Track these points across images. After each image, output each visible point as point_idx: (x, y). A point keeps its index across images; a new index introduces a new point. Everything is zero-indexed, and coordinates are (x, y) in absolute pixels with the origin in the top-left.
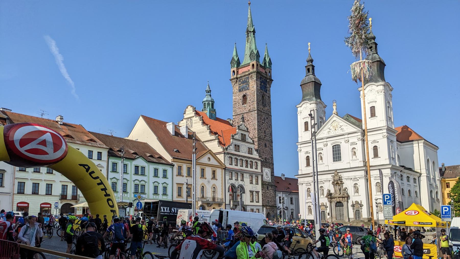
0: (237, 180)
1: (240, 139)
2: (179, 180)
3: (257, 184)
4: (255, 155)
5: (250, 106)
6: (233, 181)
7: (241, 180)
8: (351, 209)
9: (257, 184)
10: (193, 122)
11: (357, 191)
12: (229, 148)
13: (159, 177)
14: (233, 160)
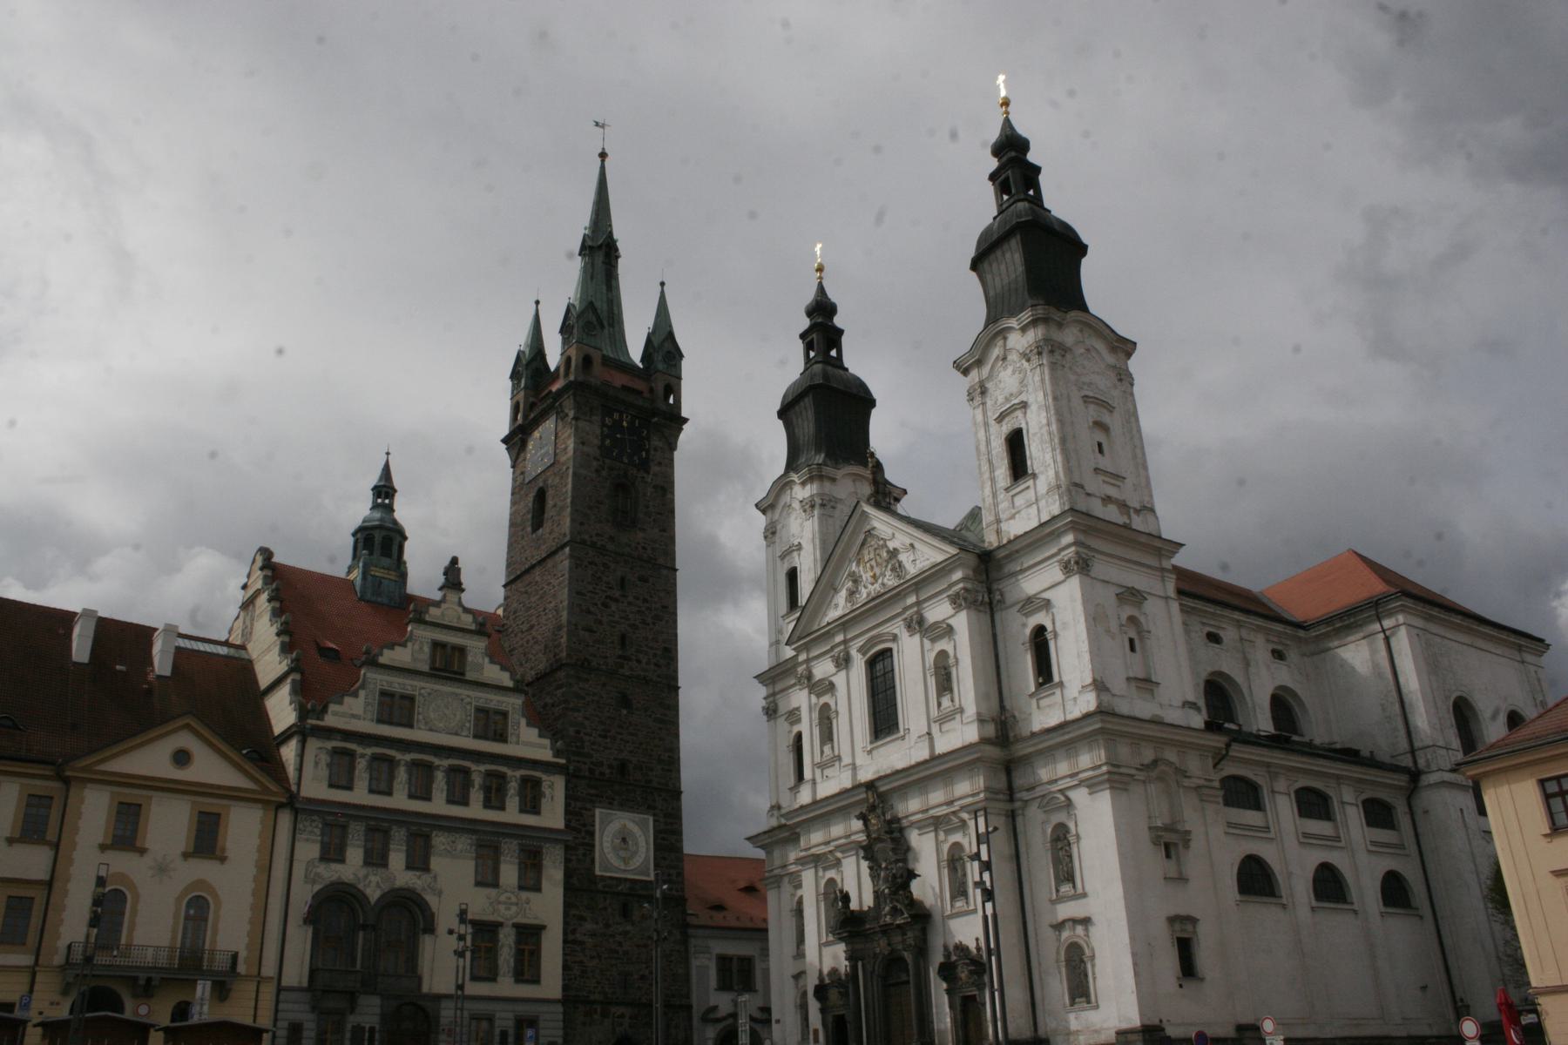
0: (376, 859)
1: (426, 668)
4: (530, 743)
6: (352, 867)
7: (410, 867)
8: (939, 992)
9: (531, 881)
12: (333, 707)
14: (361, 764)
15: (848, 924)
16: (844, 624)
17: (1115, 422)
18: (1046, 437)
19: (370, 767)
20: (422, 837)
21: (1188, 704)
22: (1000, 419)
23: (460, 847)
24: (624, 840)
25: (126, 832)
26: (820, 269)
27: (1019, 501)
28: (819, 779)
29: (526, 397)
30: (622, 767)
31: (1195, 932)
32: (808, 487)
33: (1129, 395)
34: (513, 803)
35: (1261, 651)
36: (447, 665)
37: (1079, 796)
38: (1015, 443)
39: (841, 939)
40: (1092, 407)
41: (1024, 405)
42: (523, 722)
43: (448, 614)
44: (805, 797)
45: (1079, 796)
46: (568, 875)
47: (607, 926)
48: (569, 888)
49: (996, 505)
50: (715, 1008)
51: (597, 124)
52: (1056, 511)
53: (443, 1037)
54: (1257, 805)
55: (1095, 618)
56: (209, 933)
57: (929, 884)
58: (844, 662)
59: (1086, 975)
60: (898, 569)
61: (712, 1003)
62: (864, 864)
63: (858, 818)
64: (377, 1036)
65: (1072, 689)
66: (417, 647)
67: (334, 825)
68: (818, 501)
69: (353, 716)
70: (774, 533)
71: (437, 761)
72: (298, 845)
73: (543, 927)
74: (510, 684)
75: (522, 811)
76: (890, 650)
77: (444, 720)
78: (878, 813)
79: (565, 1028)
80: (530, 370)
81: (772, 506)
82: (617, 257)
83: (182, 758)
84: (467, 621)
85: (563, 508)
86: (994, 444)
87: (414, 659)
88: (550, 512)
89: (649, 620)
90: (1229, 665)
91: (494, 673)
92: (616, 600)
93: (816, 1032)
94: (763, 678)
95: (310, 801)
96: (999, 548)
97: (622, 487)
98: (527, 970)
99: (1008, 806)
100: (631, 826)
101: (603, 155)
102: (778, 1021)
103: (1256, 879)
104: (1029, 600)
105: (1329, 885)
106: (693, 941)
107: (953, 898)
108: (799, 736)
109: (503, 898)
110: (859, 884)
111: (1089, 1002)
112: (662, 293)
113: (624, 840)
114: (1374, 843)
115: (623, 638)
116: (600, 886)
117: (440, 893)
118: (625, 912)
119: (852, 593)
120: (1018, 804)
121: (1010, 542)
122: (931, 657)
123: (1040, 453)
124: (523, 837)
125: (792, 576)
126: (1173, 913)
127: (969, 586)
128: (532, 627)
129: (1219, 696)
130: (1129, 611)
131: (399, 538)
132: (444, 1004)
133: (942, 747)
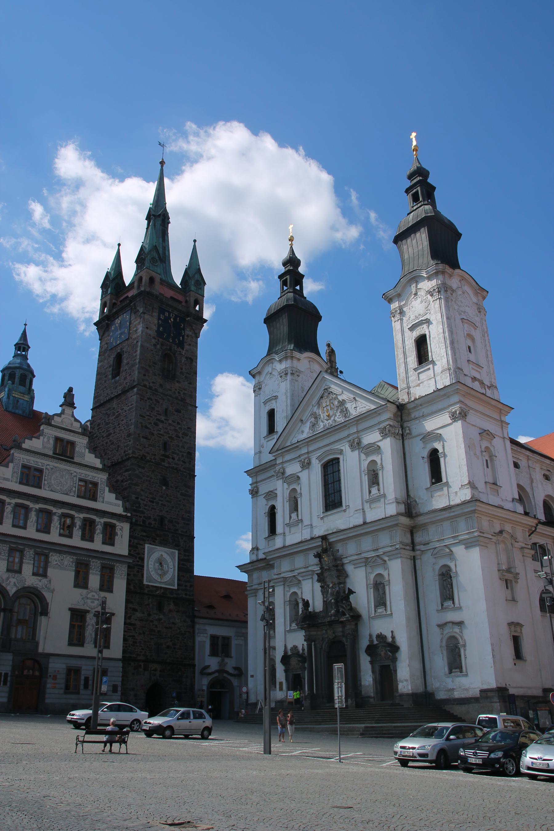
1: (51, 453)
4: (109, 502)
5: (125, 378)
8: (365, 662)
9: (107, 585)
11: (381, 601)
15: (307, 620)
17: (477, 334)
18: (442, 340)
19: (14, 511)
20: (44, 552)
21: (513, 500)
22: (412, 329)
23: (66, 563)
24: (161, 564)
26: (291, 239)
27: (423, 376)
28: (287, 534)
29: (111, 300)
30: (162, 520)
31: (521, 633)
34: (98, 537)
35: (538, 476)
36: (64, 451)
37: (459, 551)
39: (302, 629)
40: (466, 325)
42: (107, 489)
43: (66, 421)
44: (278, 542)
46: (128, 584)
47: (149, 615)
48: (128, 591)
49: (407, 378)
50: (208, 667)
52: (448, 383)
53: (50, 680)
55: (469, 447)
58: (306, 465)
59: (460, 656)
60: (345, 412)
61: (207, 664)
62: (318, 586)
63: (315, 556)
64: (9, 679)
66: (46, 440)
68: (289, 371)
70: (260, 389)
71: (54, 510)
74: (100, 466)
75: (104, 543)
76: (338, 459)
77: (60, 485)
78: (328, 556)
79: (122, 677)
81: (259, 373)
82: (169, 223)
84: (76, 427)
85: (133, 365)
87: (44, 447)
88: (124, 367)
89: (180, 435)
92: (162, 422)
93: (281, 684)
94: (249, 473)
96: (409, 403)
97: (168, 357)
99: (412, 554)
100: (165, 556)
101: (162, 163)
102: (252, 676)
104: (429, 434)
106: (197, 626)
107: (376, 607)
108: (273, 508)
109: (90, 596)
110: (313, 594)
111: (461, 672)
112: (195, 246)
113: (161, 564)
116: (146, 591)
117: (53, 591)
118: (160, 608)
119: (313, 425)
121: (416, 399)
122: (365, 464)
123: (438, 349)
124: (104, 559)
125: (271, 414)
126: (510, 621)
127: (392, 424)
128: (110, 434)
129: (522, 497)
130: (485, 444)
131: (30, 376)
132: (51, 660)
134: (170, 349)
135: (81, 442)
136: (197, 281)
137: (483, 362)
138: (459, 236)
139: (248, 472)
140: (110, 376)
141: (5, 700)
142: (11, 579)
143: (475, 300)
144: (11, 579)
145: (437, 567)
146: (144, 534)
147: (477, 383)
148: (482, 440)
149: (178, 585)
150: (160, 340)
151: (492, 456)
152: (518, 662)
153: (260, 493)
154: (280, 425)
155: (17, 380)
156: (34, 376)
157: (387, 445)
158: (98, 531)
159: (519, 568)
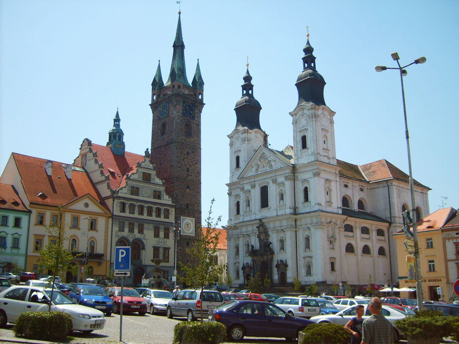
0: (131, 230)
1: (141, 180)
2: (40, 230)
3: (167, 236)
4: (166, 199)
6: (126, 233)
8: (275, 270)
9: (167, 236)
10: (88, 158)
11: (282, 248)
12: (120, 191)
13: (8, 226)
14: (127, 206)
15: (253, 252)
16: (254, 176)
17: (329, 135)
23: (150, 227)
25: (75, 225)
32: (244, 134)
33: (333, 127)
38: (304, 139)
41: (307, 130)
42: (165, 193)
45: (312, 229)
47: (184, 248)
51: (178, 2)
54: (352, 231)
56: (95, 250)
57: (275, 245)
58: (253, 187)
60: (271, 166)
62: (257, 239)
65: (313, 204)
66: (139, 174)
67: (121, 222)
69: (126, 193)
70: (232, 145)
72: (113, 227)
73: (170, 248)
74: (162, 184)
76: (267, 186)
77: (146, 195)
80: (157, 84)
83: (87, 205)
86: (298, 138)
87: (139, 177)
89: (194, 164)
90: (348, 192)
91: (158, 181)
95: (116, 216)
98: (166, 259)
99: (295, 229)
101: (180, 13)
103: (350, 249)
105: (366, 250)
108: (238, 202)
109: (160, 241)
110: (255, 242)
111: (311, 275)
112: (198, 62)
114: (378, 240)
115: (188, 169)
119: (257, 170)
120: (297, 229)
125: (238, 158)
126: (331, 257)
128: (162, 164)
132: (147, 267)
133: (280, 213)
134: (189, 121)
135: (153, 173)
136: (200, 83)
137: (330, 148)
138: (325, 83)
139: (227, 185)
140: (160, 134)
141: (132, 283)
142: (130, 235)
143: (329, 117)
144: (130, 235)
145: (304, 235)
146: (180, 212)
147: (326, 158)
148: (326, 184)
149: (195, 234)
150: (184, 117)
151: (330, 190)
152: (332, 272)
153: (232, 195)
154: (242, 164)
155: (117, 138)
156: (124, 135)
157: (288, 184)
158: (162, 213)
159: (337, 236)
